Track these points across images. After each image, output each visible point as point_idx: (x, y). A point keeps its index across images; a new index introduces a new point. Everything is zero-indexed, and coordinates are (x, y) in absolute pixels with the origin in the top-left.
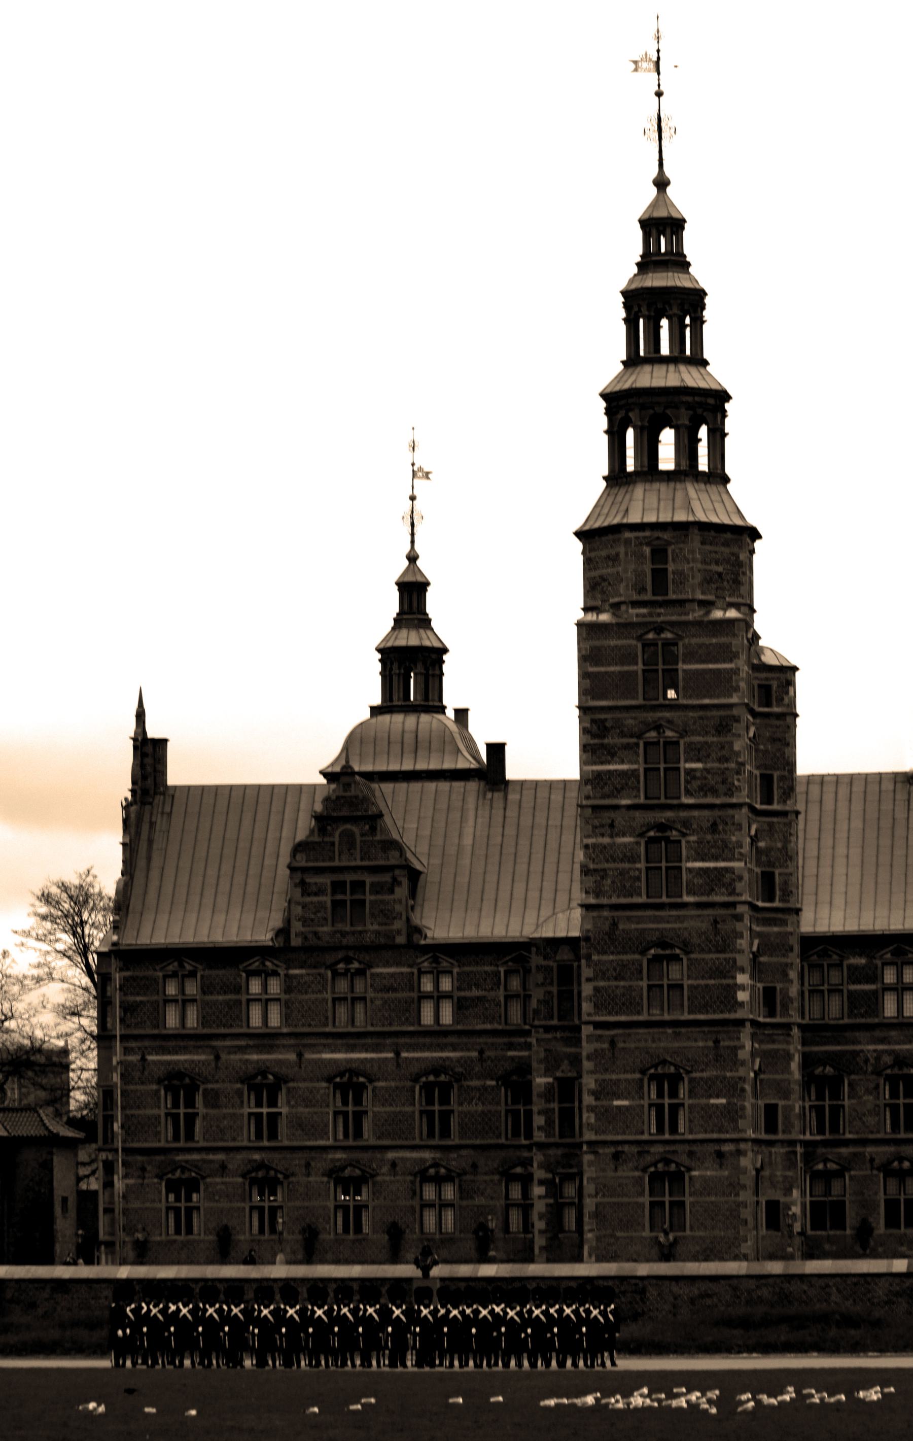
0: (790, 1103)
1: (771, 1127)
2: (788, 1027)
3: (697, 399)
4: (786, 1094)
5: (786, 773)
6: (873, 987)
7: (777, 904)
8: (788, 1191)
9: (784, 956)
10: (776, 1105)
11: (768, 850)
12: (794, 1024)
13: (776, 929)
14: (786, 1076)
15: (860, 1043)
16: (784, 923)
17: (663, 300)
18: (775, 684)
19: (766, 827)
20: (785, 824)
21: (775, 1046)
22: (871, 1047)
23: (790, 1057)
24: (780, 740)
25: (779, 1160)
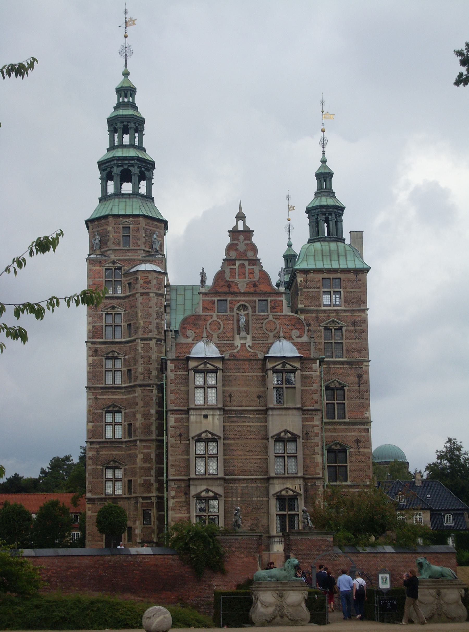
0: (136, 478)
2: (136, 441)
3: (107, 164)
5: (136, 321)
8: (135, 522)
9: (135, 408)
10: (131, 480)
12: (137, 440)
13: (132, 396)
14: (134, 466)
16: (134, 392)
17: (126, 123)
18: (132, 281)
21: (131, 452)
23: (136, 456)
24: (133, 306)
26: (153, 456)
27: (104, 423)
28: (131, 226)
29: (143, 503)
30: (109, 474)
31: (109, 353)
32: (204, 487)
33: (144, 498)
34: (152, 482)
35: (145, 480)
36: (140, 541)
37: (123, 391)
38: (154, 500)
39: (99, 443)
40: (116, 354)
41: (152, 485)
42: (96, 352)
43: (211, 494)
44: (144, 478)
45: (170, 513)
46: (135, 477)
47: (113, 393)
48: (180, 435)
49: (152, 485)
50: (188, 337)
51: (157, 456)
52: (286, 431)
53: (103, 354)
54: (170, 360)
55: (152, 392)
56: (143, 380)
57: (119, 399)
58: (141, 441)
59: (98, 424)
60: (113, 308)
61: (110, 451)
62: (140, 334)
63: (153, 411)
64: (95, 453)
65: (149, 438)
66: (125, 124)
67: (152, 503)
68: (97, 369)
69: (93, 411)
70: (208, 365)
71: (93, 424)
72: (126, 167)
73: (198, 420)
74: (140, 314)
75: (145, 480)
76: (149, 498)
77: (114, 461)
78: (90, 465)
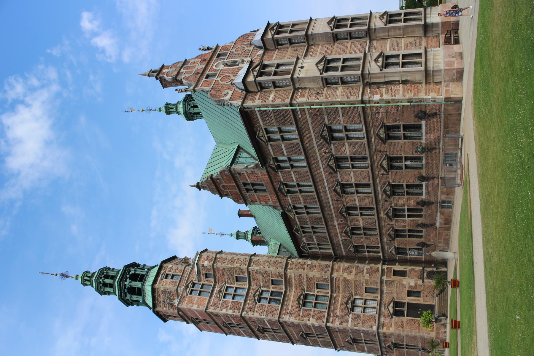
0: (364, 281)
1: (375, 291)
2: (332, 279)
4: (361, 283)
6: (314, 237)
7: (283, 279)
8: (403, 286)
9: (303, 278)
11: (263, 281)
13: (293, 281)
14: (353, 282)
15: (339, 242)
16: (290, 277)
18: (204, 272)
19: (255, 281)
20: (253, 273)
21: (341, 286)
22: (340, 238)
23: (345, 280)
25: (389, 289)
26: (347, 265)
27: (313, 309)
28: (167, 272)
29: (387, 276)
30: (358, 310)
31: (254, 298)
32: (373, 63)
33: (382, 274)
34: (369, 267)
35: (367, 273)
36: (421, 281)
37: (288, 291)
38: (385, 267)
39: (329, 315)
40: (258, 293)
41: (371, 268)
42: (250, 309)
43: (380, 59)
44: (365, 274)
45: (397, 97)
46: (363, 283)
47: (289, 298)
48: (318, 94)
49: (371, 268)
50: (228, 93)
51: (346, 262)
52: (329, 23)
53: (254, 303)
54: (243, 103)
55: (293, 262)
56: (282, 267)
57: (294, 295)
58: (332, 273)
59: (312, 314)
60: (220, 291)
61: (337, 306)
62: (244, 267)
63: (309, 262)
64: (337, 319)
65: (331, 267)
66: (103, 276)
67: (387, 268)
68: (266, 310)
69: (300, 317)
70: (256, 69)
71: (311, 318)
72: (128, 276)
73: (305, 72)
74: (230, 266)
75: (367, 273)
76: (383, 270)
77: (347, 303)
78: (347, 325)
